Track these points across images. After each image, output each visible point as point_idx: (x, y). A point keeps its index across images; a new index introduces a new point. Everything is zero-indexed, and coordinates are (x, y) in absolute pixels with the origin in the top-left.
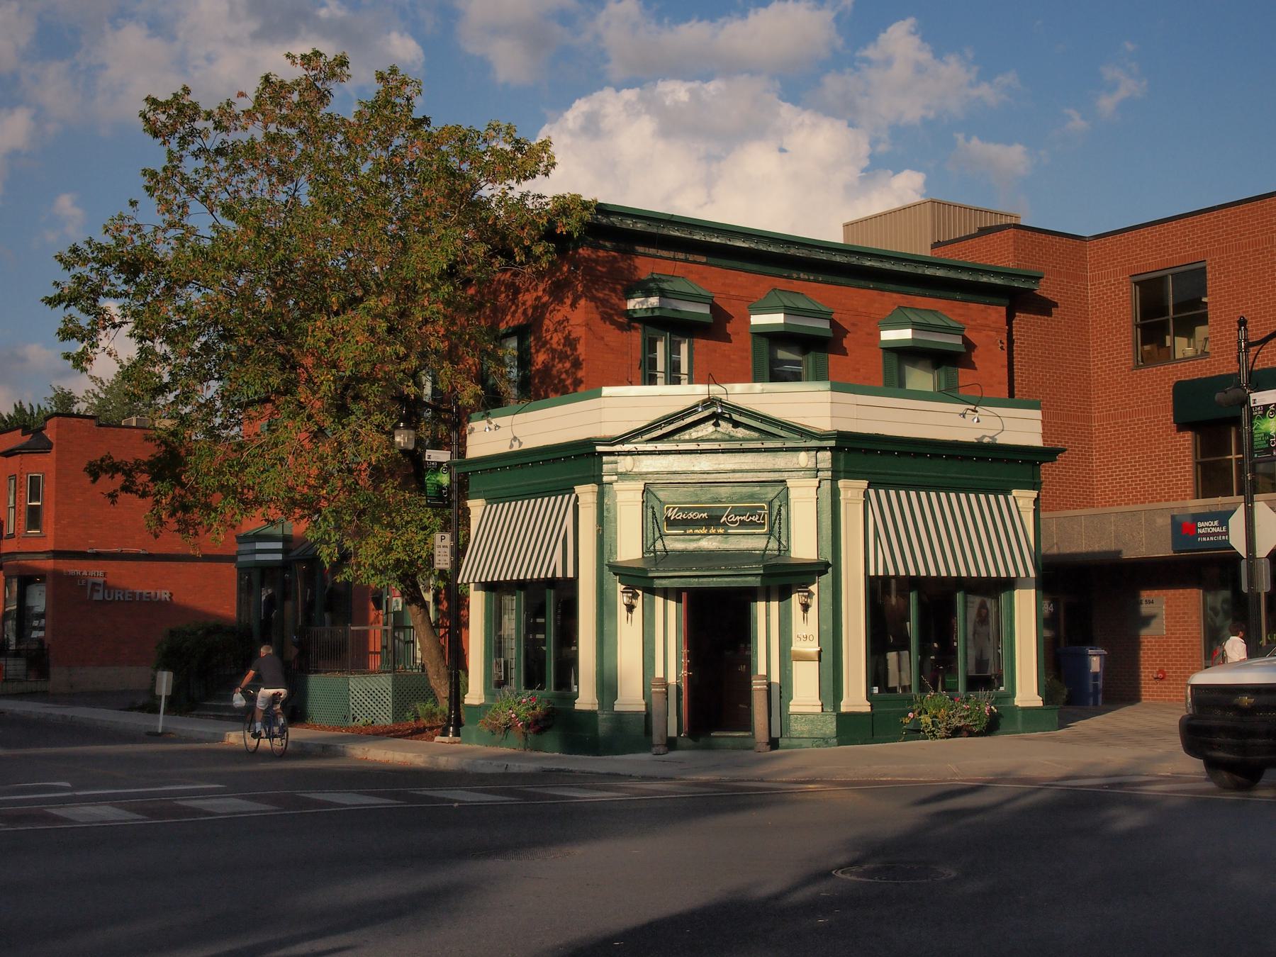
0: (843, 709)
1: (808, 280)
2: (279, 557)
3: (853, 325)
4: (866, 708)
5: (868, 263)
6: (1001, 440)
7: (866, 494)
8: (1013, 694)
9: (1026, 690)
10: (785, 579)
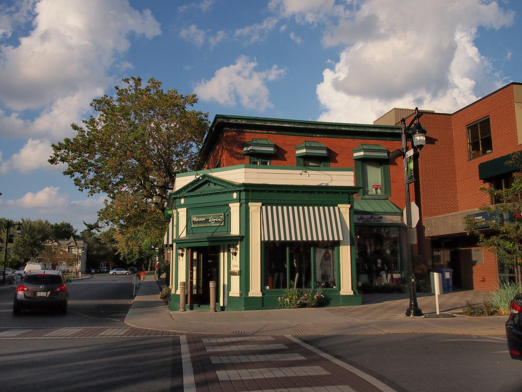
0: (230, 295)
1: (321, 137)
2: (165, 243)
3: (341, 152)
4: (260, 295)
5: (344, 129)
6: (331, 184)
7: (261, 208)
8: (340, 289)
9: (346, 287)
10: (230, 243)
